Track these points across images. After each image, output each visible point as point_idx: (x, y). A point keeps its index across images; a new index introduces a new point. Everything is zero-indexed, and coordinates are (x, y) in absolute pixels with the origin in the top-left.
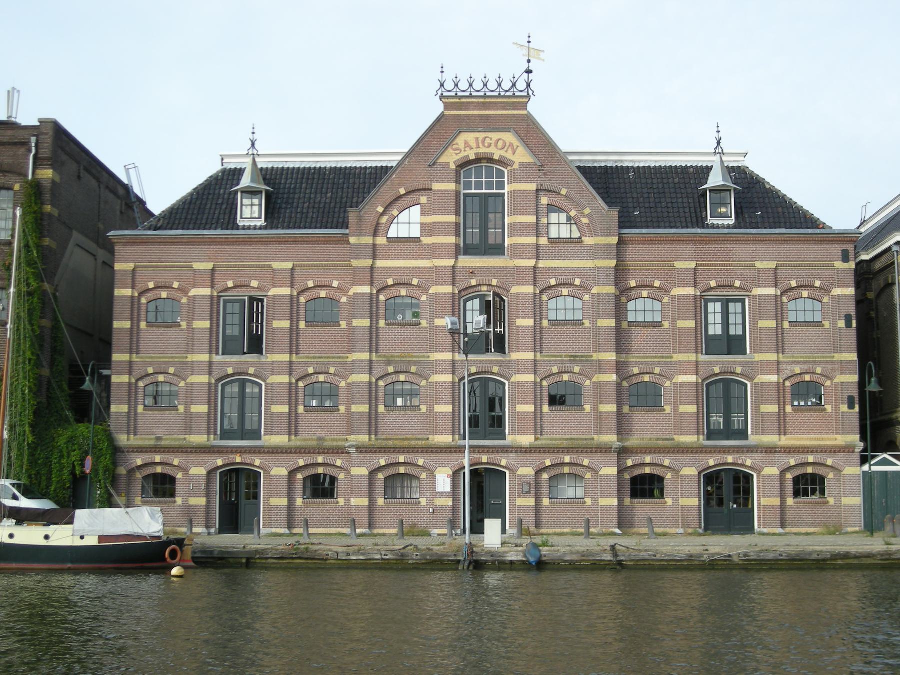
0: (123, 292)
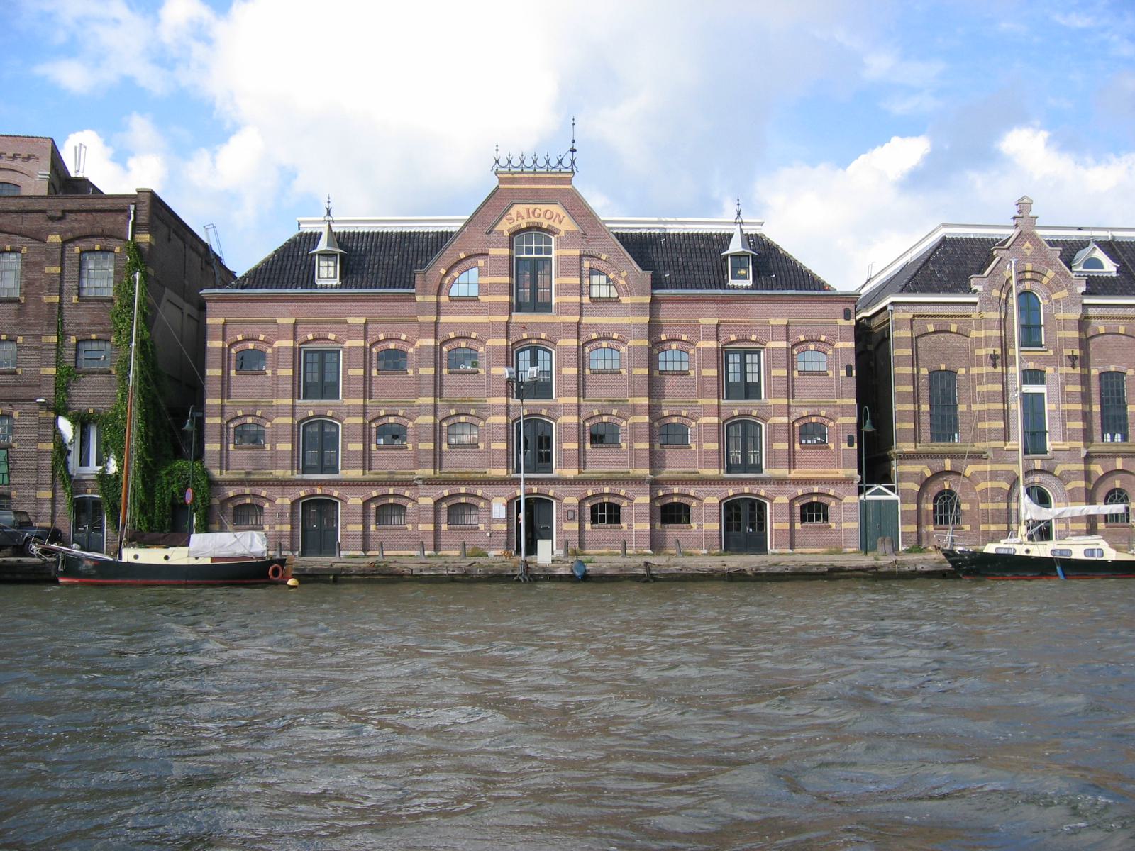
0: (214, 344)
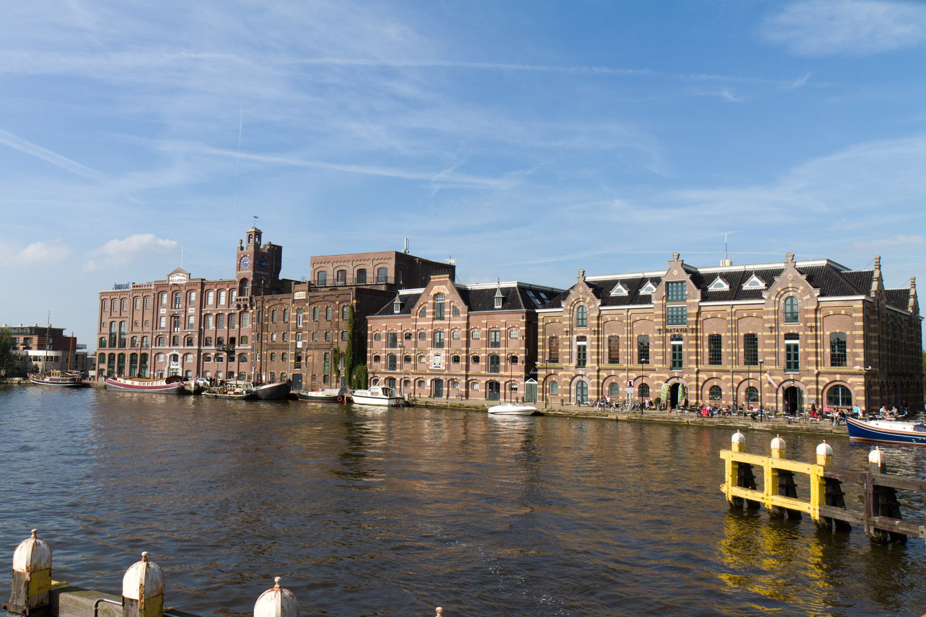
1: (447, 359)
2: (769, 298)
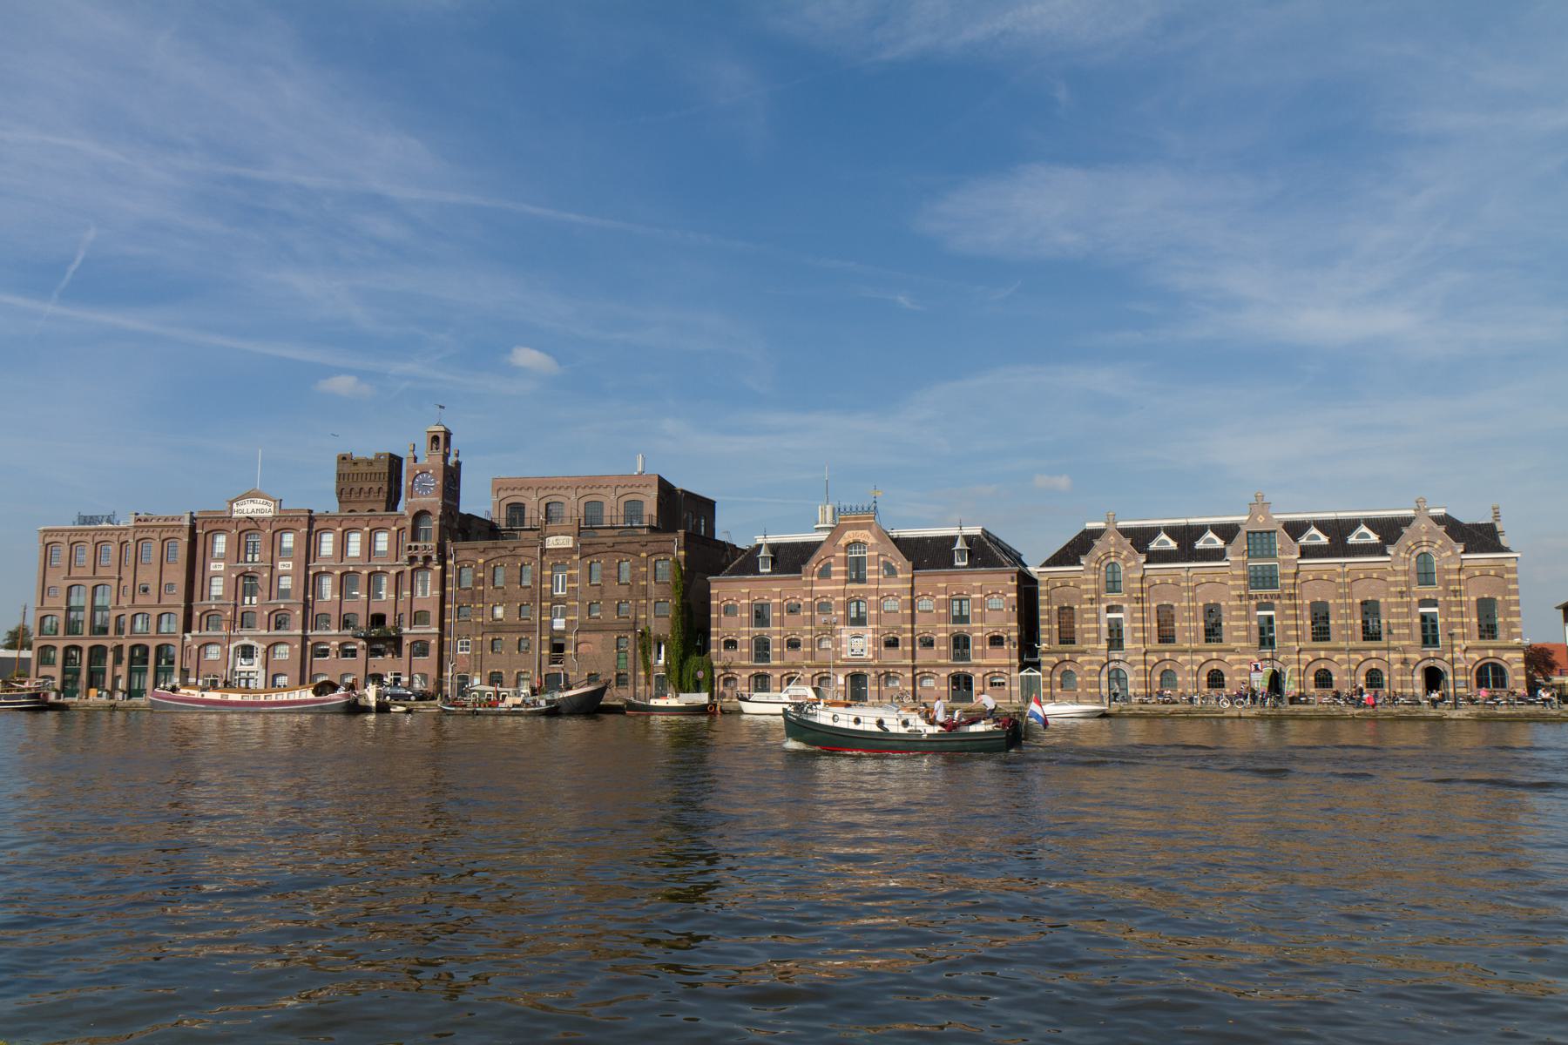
0: (714, 602)
1: (876, 642)
2: (1397, 554)
